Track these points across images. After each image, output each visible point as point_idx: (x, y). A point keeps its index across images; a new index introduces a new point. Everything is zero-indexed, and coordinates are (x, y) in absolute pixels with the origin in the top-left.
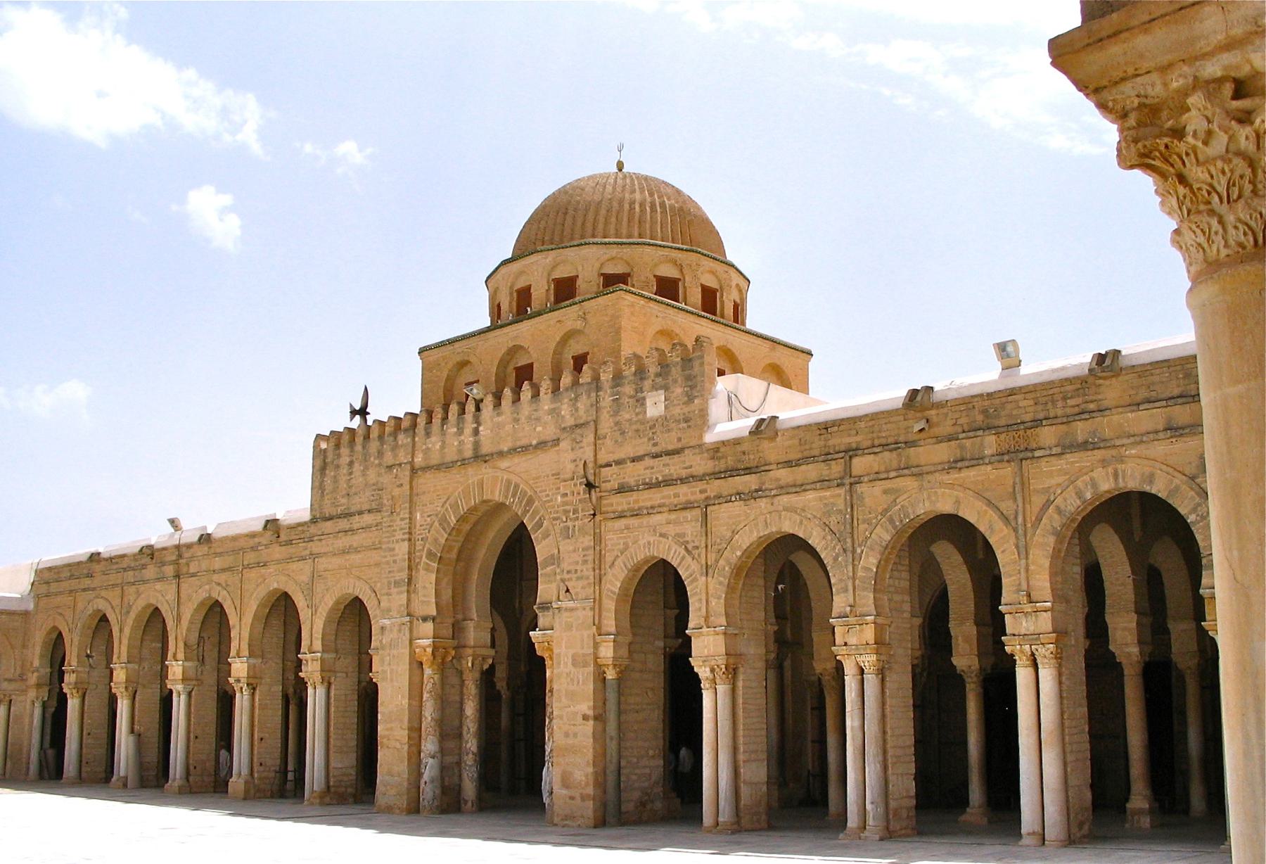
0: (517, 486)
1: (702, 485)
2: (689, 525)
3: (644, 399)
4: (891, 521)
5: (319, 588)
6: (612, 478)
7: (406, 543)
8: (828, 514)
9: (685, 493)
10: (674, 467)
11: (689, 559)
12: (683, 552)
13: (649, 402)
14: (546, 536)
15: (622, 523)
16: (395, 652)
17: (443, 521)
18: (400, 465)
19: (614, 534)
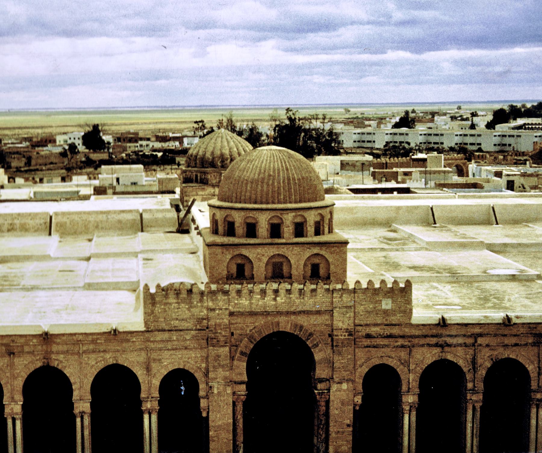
0: (301, 327)
1: (410, 339)
2: (403, 354)
3: (381, 301)
4: (492, 359)
5: (154, 366)
6: (363, 331)
7: (227, 349)
8: (466, 355)
9: (400, 342)
10: (395, 331)
11: (402, 367)
12: (399, 363)
13: (383, 303)
14: (320, 351)
15: (367, 349)
16: (222, 398)
17: (251, 338)
18: (221, 309)
19: (361, 354)
